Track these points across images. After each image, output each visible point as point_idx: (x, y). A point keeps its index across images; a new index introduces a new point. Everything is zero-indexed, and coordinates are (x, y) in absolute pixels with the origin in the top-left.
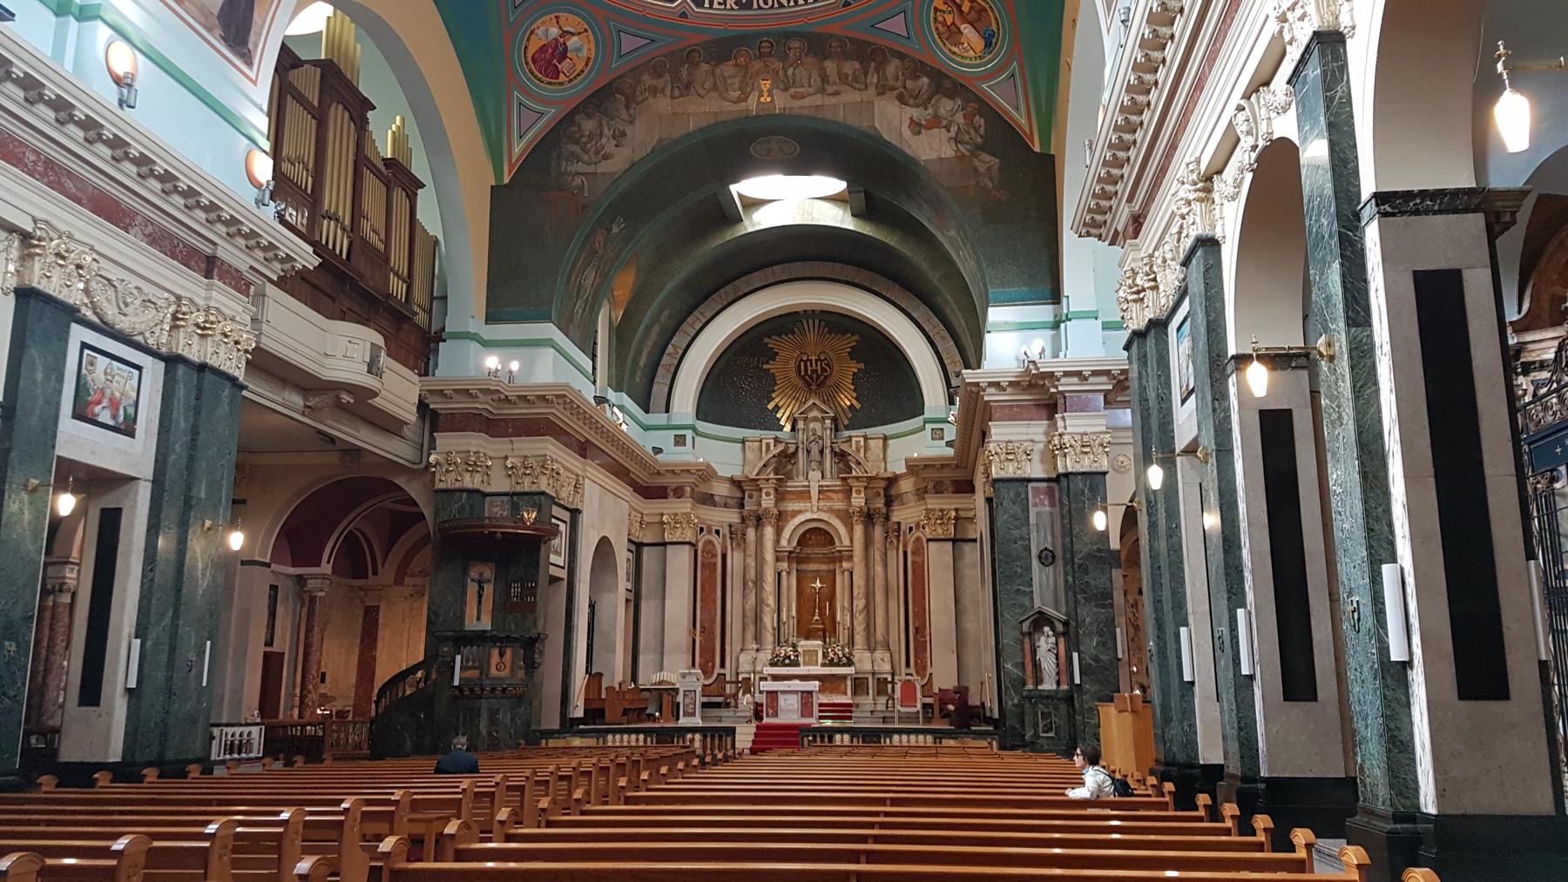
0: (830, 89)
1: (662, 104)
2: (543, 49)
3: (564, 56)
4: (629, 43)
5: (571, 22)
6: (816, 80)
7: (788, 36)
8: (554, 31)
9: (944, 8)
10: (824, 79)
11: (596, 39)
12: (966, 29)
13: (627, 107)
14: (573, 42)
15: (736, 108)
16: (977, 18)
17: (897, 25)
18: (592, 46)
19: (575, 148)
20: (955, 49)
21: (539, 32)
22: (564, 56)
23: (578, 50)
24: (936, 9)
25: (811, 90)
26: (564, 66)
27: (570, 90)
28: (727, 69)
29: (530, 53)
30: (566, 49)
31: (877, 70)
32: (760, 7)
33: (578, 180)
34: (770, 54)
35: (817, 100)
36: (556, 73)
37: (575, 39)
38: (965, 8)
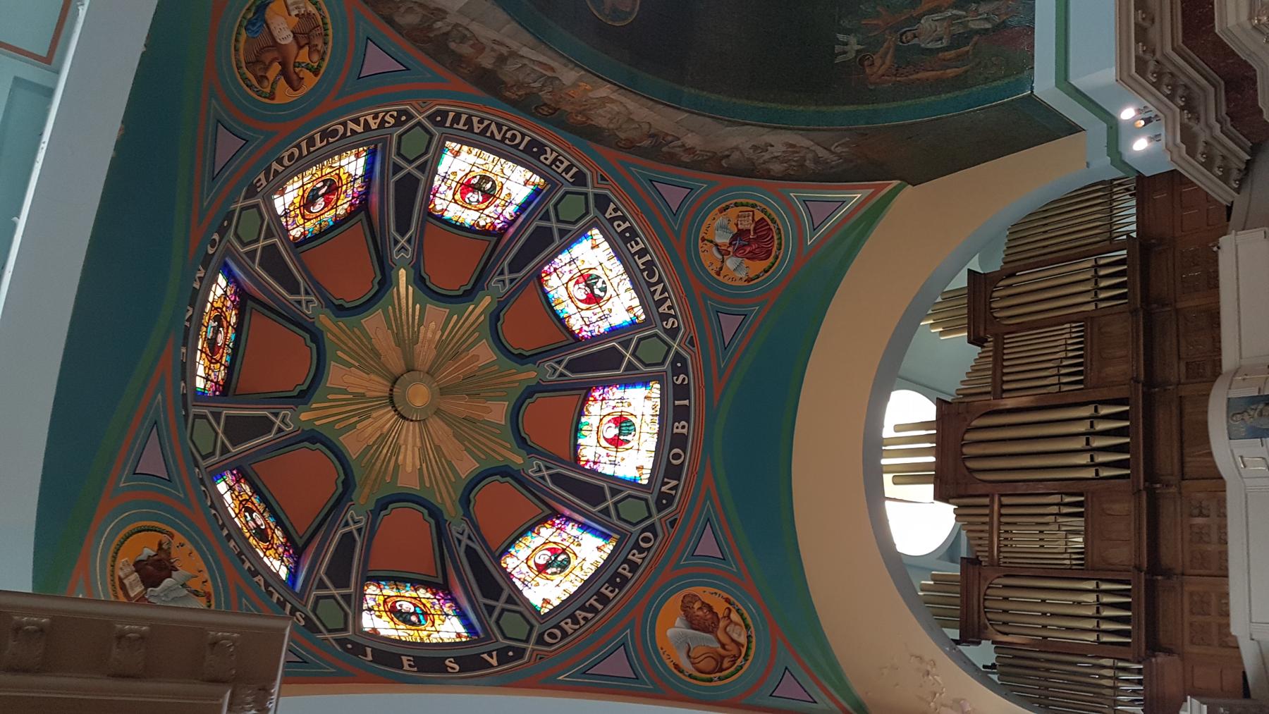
0: (504, 51)
1: (691, 140)
2: (753, 257)
3: (741, 234)
4: (674, 196)
5: (710, 258)
6: (511, 67)
7: (514, 103)
8: (731, 263)
9: (306, 74)
10: (502, 59)
11: (701, 222)
12: (284, 36)
13: (728, 156)
14: (723, 239)
15: (623, 99)
16: (264, 52)
17: (377, 61)
18: (708, 221)
19: (807, 163)
20: (311, 9)
21: (743, 275)
22: (741, 234)
23: (723, 227)
24: (316, 72)
25: (526, 62)
26: (747, 224)
27: (765, 199)
28: (601, 122)
29: (765, 264)
30: (734, 238)
31: (430, 28)
32: (523, 135)
33: (839, 150)
34: (545, 104)
35: (524, 51)
36: (761, 226)
37: (718, 241)
38: (276, 67)
